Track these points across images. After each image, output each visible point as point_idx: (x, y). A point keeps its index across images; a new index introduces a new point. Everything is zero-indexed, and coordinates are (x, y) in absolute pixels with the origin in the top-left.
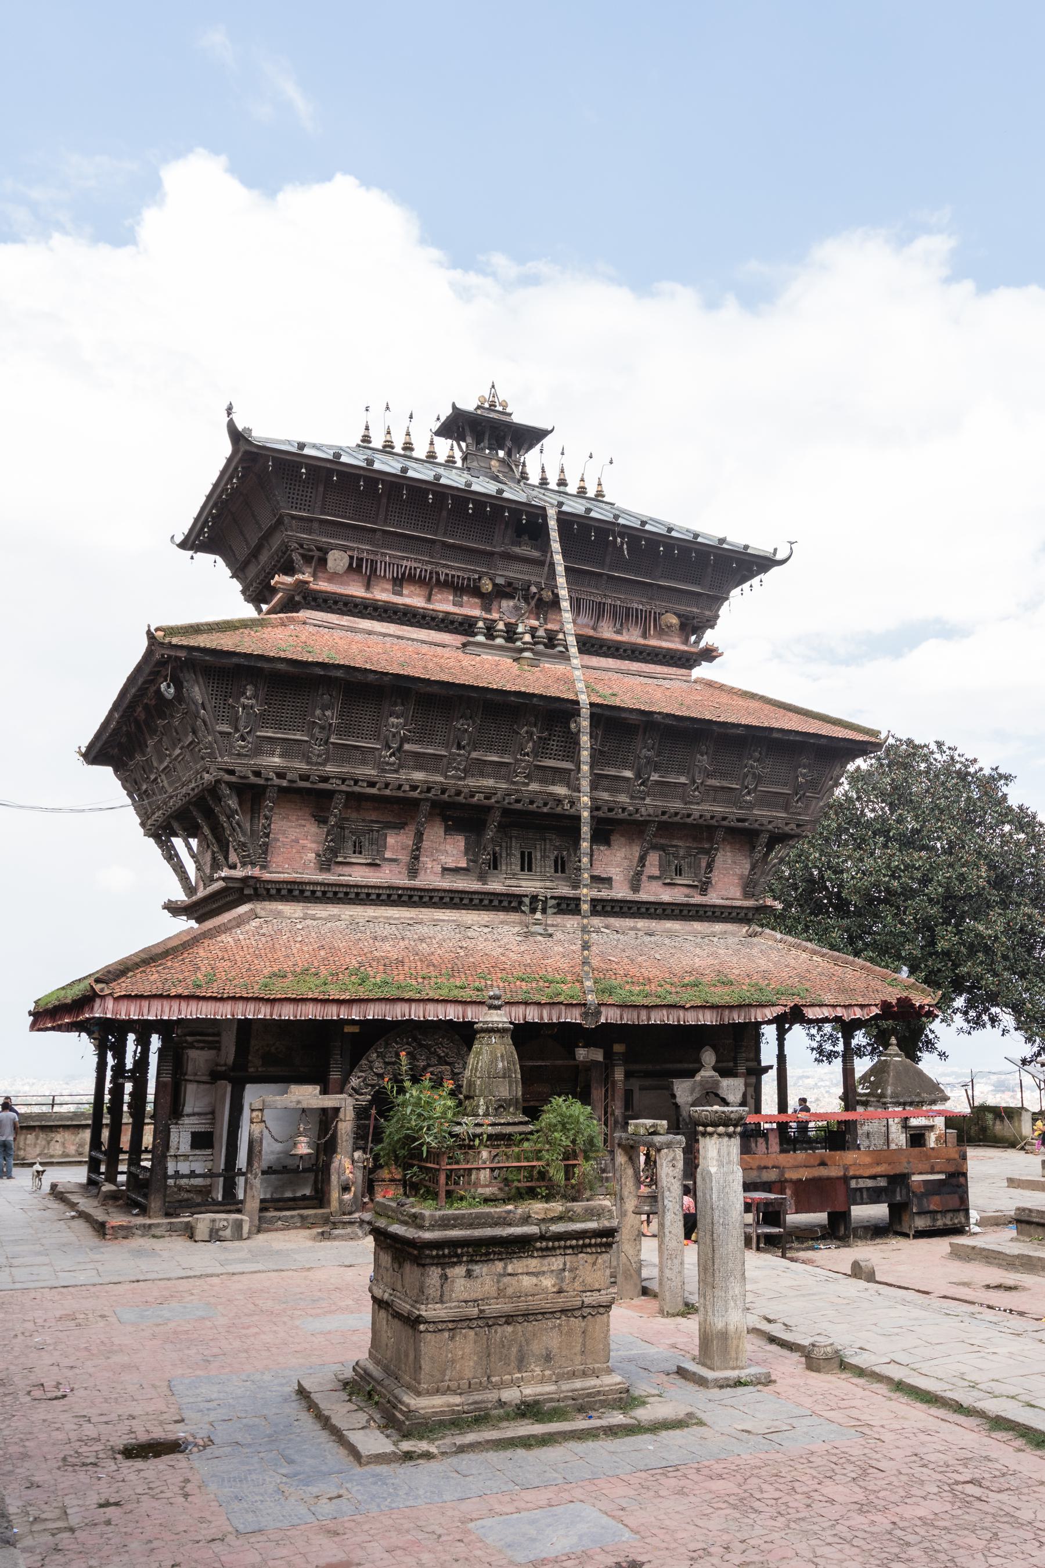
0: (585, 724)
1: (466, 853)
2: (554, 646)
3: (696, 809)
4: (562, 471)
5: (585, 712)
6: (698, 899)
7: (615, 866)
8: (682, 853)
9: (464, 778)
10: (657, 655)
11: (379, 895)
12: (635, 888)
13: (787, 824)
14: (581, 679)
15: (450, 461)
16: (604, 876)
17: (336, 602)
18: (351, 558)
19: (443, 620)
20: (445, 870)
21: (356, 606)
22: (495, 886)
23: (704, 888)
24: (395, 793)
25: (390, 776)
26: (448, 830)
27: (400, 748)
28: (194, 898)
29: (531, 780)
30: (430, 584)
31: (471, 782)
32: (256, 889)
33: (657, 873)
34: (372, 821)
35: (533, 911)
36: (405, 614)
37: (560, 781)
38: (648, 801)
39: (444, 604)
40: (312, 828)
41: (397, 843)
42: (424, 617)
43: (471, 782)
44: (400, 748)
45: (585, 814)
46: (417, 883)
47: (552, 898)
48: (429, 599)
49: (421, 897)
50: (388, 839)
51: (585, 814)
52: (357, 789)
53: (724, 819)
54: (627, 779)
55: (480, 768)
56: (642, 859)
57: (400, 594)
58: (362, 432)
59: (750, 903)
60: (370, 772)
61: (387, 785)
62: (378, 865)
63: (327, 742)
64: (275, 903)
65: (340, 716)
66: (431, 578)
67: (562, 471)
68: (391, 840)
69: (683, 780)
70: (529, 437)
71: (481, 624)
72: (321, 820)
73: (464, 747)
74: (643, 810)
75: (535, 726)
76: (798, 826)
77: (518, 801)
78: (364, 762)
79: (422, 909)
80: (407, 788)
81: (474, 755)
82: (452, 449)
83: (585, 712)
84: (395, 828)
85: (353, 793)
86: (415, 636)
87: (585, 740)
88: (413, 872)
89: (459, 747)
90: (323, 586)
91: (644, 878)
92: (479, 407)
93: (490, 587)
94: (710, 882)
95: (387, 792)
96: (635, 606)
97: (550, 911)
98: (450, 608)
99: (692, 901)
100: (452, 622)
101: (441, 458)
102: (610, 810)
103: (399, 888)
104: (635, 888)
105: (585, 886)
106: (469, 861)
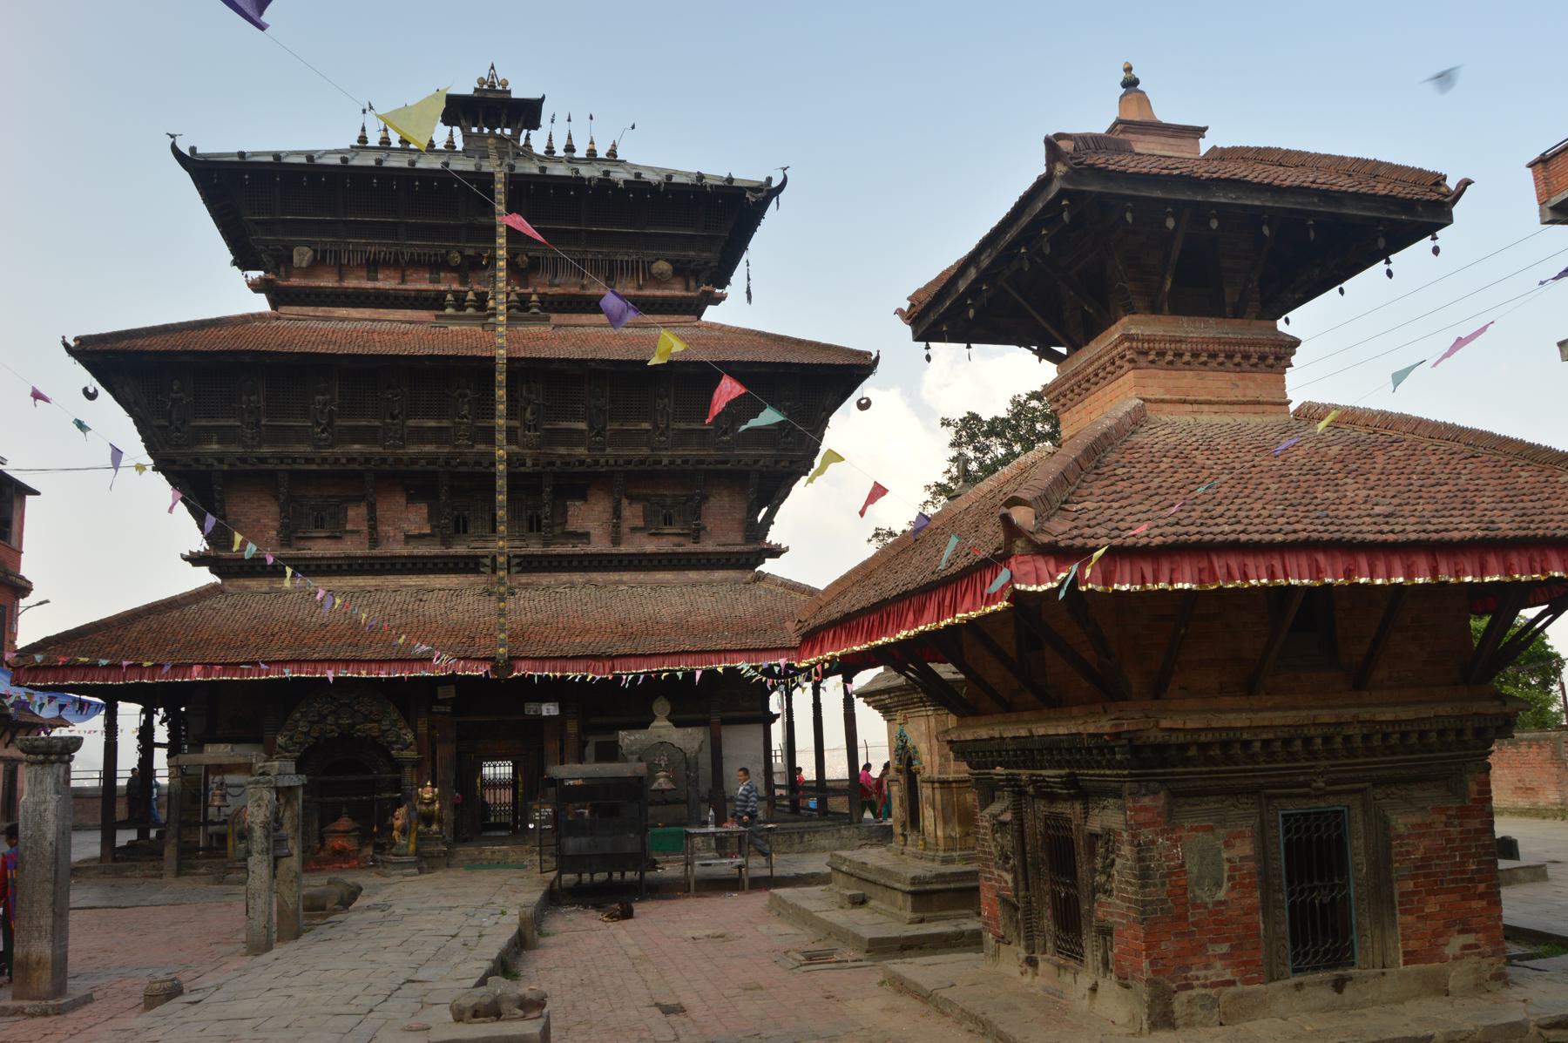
0: (501, 377)
1: (430, 518)
2: (528, 309)
3: (665, 456)
4: (570, 137)
5: (501, 365)
6: (690, 547)
7: (591, 520)
8: (668, 501)
9: (403, 447)
10: (653, 304)
11: (339, 566)
12: (616, 541)
13: (777, 462)
14: (501, 340)
15: (450, 145)
16: (581, 531)
17: (308, 296)
18: (315, 251)
19: (416, 298)
20: (409, 538)
21: (327, 296)
22: (460, 549)
23: (697, 540)
24: (335, 467)
25: (326, 452)
26: (411, 499)
27: (330, 424)
29: (475, 442)
30: (401, 265)
31: (413, 449)
33: (641, 524)
35: (494, 571)
36: (377, 297)
38: (609, 451)
39: (420, 283)
40: (274, 509)
41: (356, 515)
42: (397, 297)
43: (413, 449)
44: (330, 424)
45: (501, 467)
46: (376, 552)
47: (515, 556)
48: (403, 281)
49: (382, 565)
51: (501, 467)
52: (297, 467)
53: (702, 462)
54: (582, 431)
55: (420, 435)
56: (617, 513)
57: (376, 279)
58: (359, 133)
59: (750, 548)
60: (304, 449)
61: (324, 460)
62: (340, 538)
63: (257, 424)
66: (396, 260)
67: (570, 137)
68: (351, 513)
69: (646, 426)
70: (529, 113)
71: (449, 297)
72: (276, 498)
74: (602, 461)
76: (791, 462)
77: (460, 464)
78: (300, 441)
80: (344, 461)
81: (411, 423)
82: (451, 134)
83: (501, 365)
85: (299, 471)
86: (391, 317)
87: (501, 393)
88: (374, 542)
89: (393, 417)
90: (295, 282)
91: (625, 528)
92: (476, 90)
93: (459, 260)
94: (704, 528)
95: (327, 467)
96: (619, 258)
97: (514, 570)
98: (424, 286)
99: (680, 550)
100: (426, 299)
101: (440, 146)
102: (568, 464)
104: (616, 541)
105: (502, 538)
106: (433, 527)
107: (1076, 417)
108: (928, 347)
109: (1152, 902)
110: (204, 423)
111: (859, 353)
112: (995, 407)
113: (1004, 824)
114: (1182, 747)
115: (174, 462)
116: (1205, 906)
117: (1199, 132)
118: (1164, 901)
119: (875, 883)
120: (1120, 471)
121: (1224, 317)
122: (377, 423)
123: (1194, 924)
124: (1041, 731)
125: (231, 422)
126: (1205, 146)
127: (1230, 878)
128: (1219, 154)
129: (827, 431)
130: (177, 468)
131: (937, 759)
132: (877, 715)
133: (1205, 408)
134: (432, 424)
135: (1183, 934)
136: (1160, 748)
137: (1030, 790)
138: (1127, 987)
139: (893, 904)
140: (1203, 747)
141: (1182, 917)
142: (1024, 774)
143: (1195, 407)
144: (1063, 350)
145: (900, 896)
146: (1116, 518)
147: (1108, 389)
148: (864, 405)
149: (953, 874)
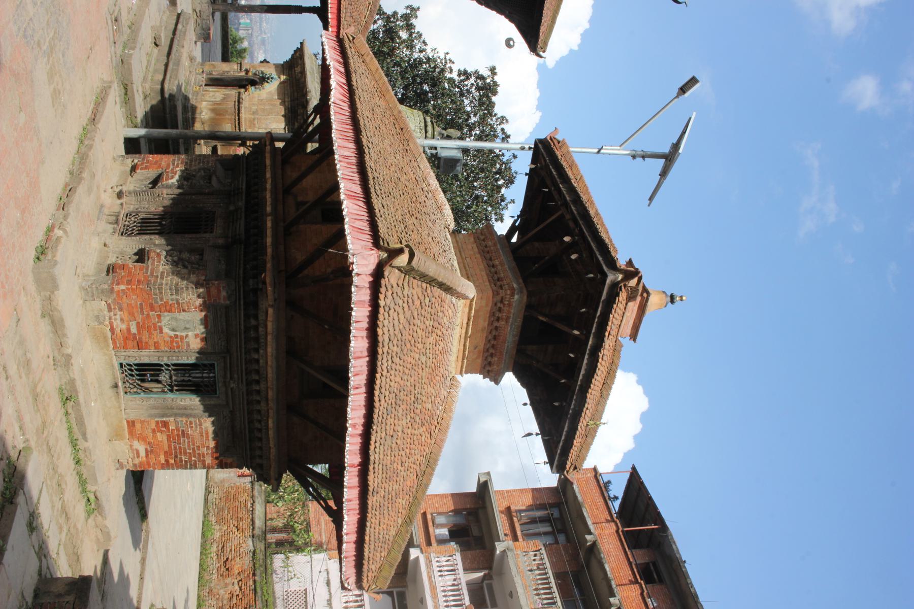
107: (470, 247)
108: (530, 148)
109: (161, 293)
111: (546, 44)
112: (501, 104)
113: (210, 179)
114: (256, 317)
116: (160, 321)
117: (634, 336)
118: (162, 299)
119: (169, 54)
120: (427, 300)
121: (518, 345)
123: (148, 315)
124: (269, 224)
126: (626, 341)
127: (176, 336)
128: (617, 349)
129: (494, 12)
131: (254, 108)
132: (288, 57)
133: (464, 331)
135: (142, 309)
136: (256, 305)
137: (232, 208)
138: (108, 271)
139: (156, 71)
140: (256, 328)
141: (152, 308)
142: (241, 204)
143: (465, 325)
144: (514, 240)
145: (161, 77)
146: (397, 308)
147: (484, 273)
148: (509, 43)
149: (176, 116)
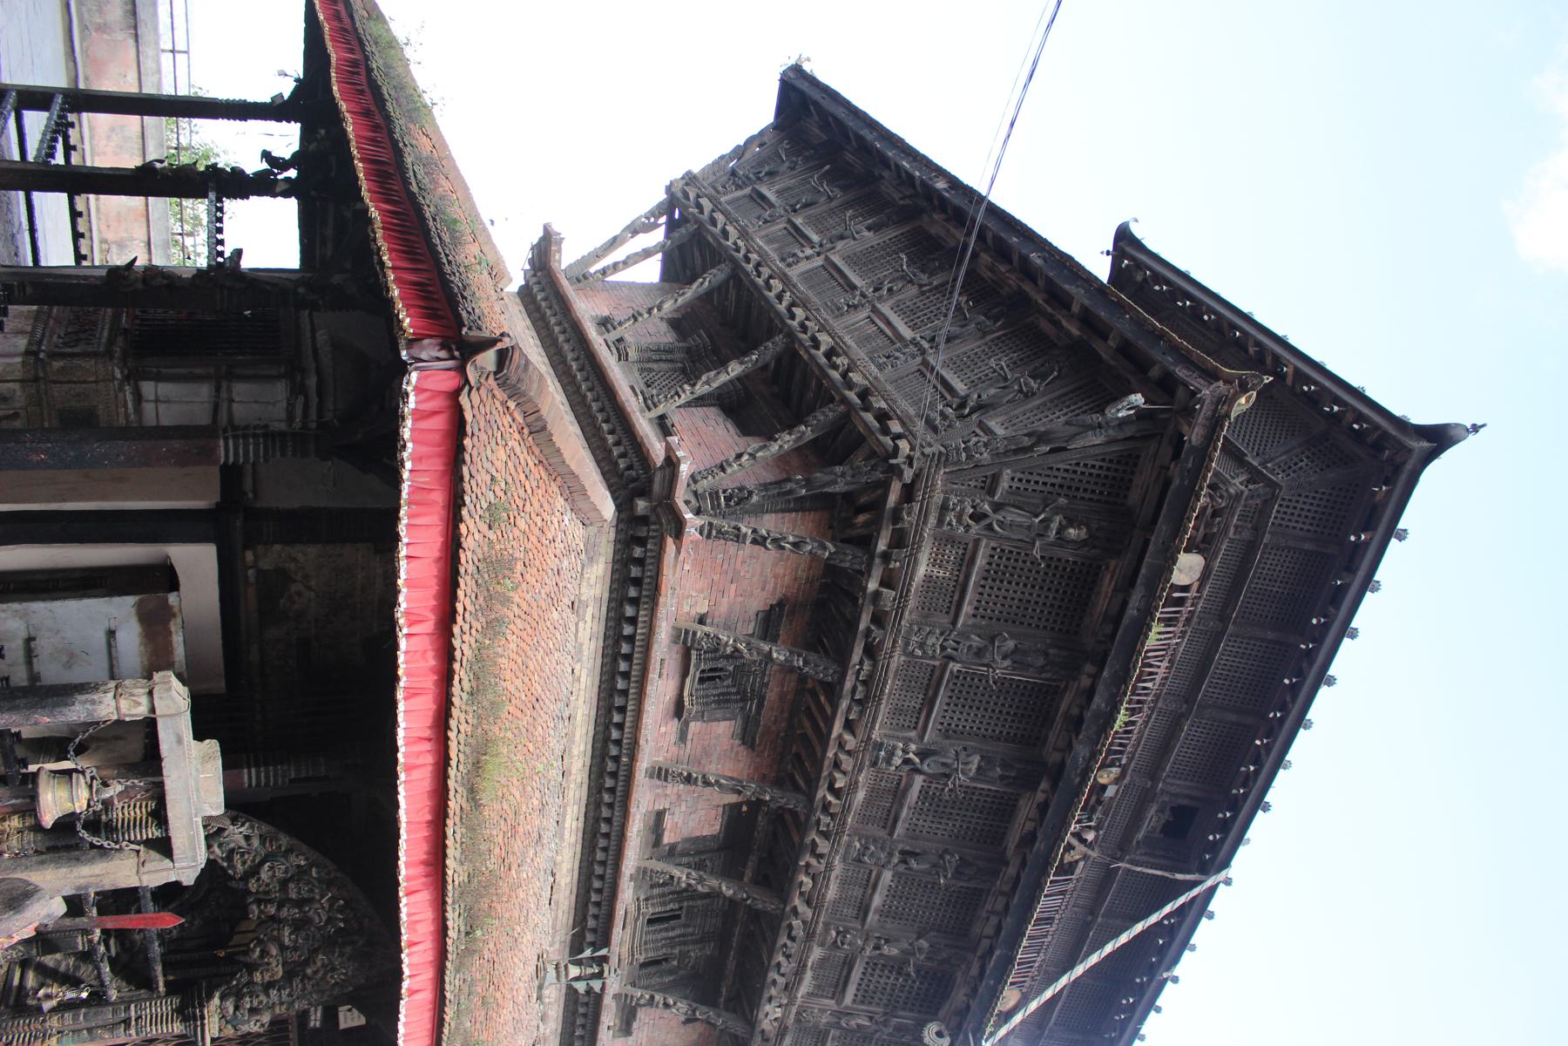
9: (844, 860)
20: (660, 815)
28: (565, 283)
32: (644, 520)
34: (762, 699)
37: (818, 987)
50: (724, 724)
64: (610, 550)
65: (1001, 682)
73: (904, 861)
75: (928, 959)
79: (585, 787)
81: (887, 876)
84: (744, 729)
88: (660, 774)
103: (633, 758)
106: (673, 847)
110: (980, 561)
115: (908, 493)
122: (900, 830)
125: (967, 608)
130: (893, 499)
134: (877, 901)
